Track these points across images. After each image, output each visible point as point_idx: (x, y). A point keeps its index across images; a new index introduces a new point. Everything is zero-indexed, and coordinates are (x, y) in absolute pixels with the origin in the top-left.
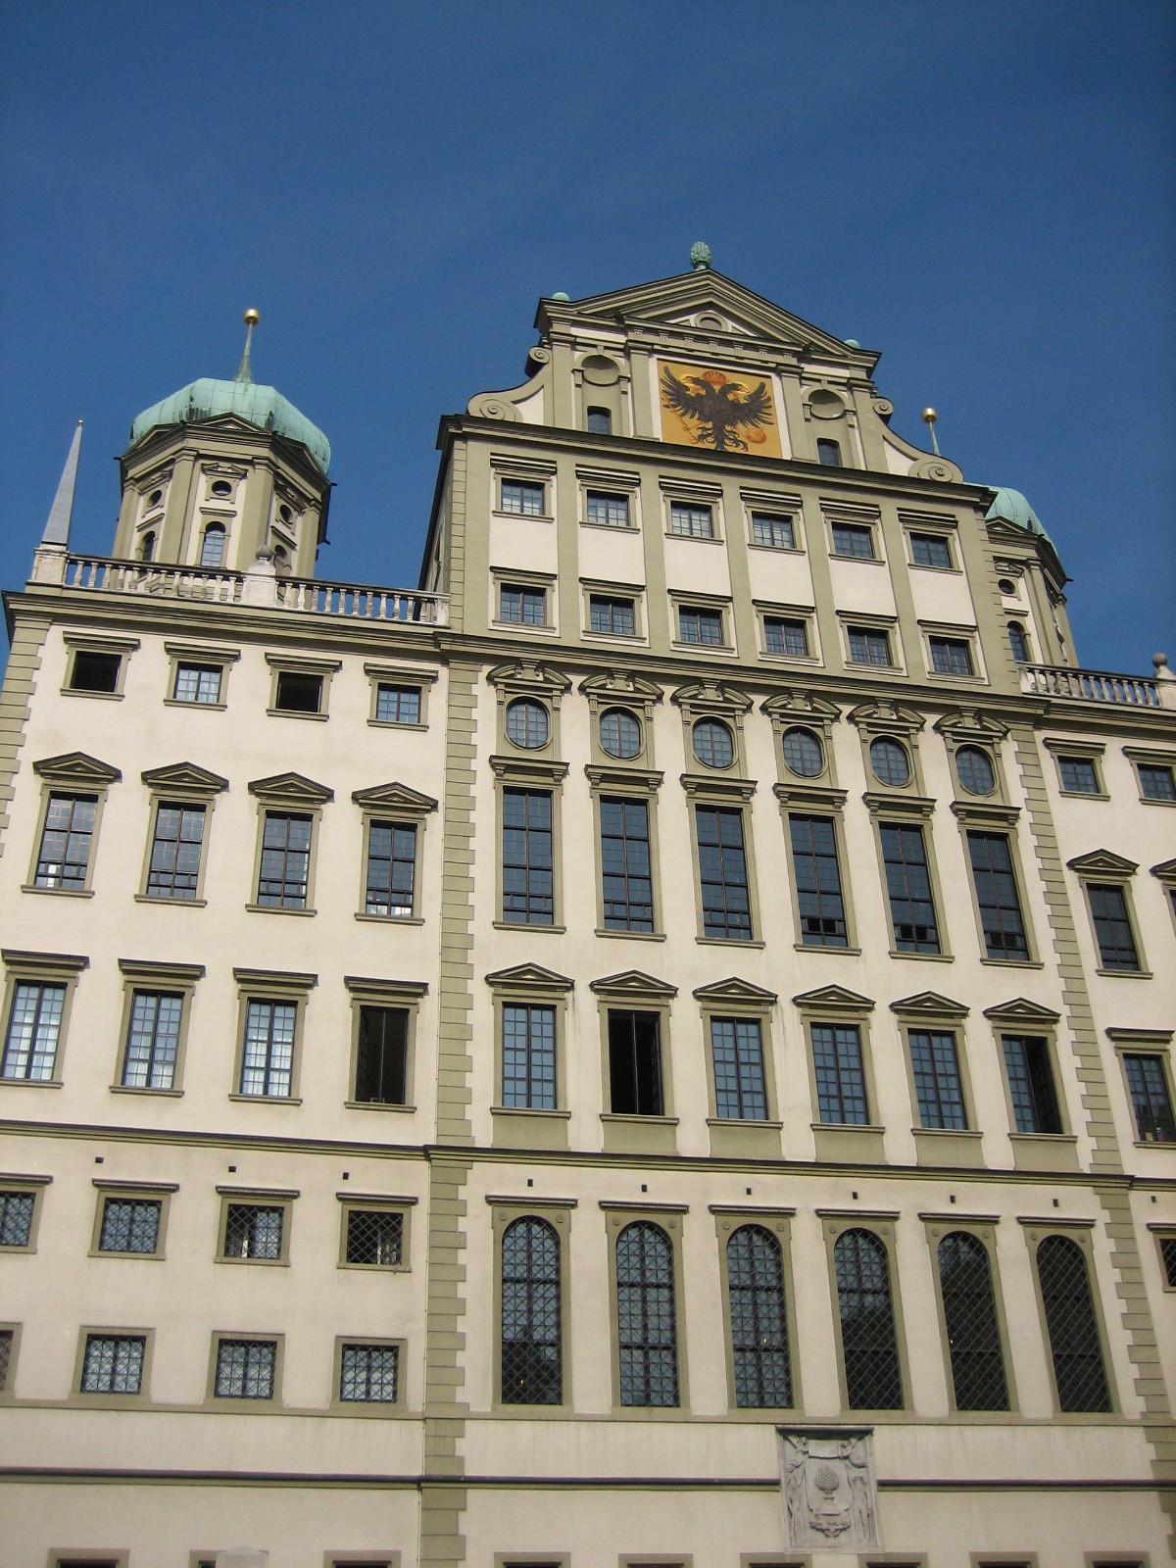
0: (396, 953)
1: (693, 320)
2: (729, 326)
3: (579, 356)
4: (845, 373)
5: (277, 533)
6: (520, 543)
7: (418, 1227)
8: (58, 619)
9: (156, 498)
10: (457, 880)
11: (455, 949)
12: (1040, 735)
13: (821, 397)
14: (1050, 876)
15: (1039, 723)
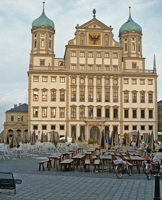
0: (63, 104)
1: (92, 27)
2: (97, 27)
3: (80, 33)
4: (109, 31)
5: (49, 40)
6: (73, 60)
7: (65, 126)
8: (32, 74)
9: (36, 35)
10: (68, 97)
11: (67, 103)
12: (123, 77)
13: (106, 34)
14: (121, 92)
15: (123, 76)
